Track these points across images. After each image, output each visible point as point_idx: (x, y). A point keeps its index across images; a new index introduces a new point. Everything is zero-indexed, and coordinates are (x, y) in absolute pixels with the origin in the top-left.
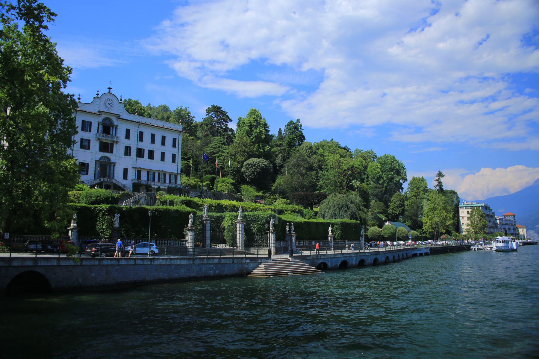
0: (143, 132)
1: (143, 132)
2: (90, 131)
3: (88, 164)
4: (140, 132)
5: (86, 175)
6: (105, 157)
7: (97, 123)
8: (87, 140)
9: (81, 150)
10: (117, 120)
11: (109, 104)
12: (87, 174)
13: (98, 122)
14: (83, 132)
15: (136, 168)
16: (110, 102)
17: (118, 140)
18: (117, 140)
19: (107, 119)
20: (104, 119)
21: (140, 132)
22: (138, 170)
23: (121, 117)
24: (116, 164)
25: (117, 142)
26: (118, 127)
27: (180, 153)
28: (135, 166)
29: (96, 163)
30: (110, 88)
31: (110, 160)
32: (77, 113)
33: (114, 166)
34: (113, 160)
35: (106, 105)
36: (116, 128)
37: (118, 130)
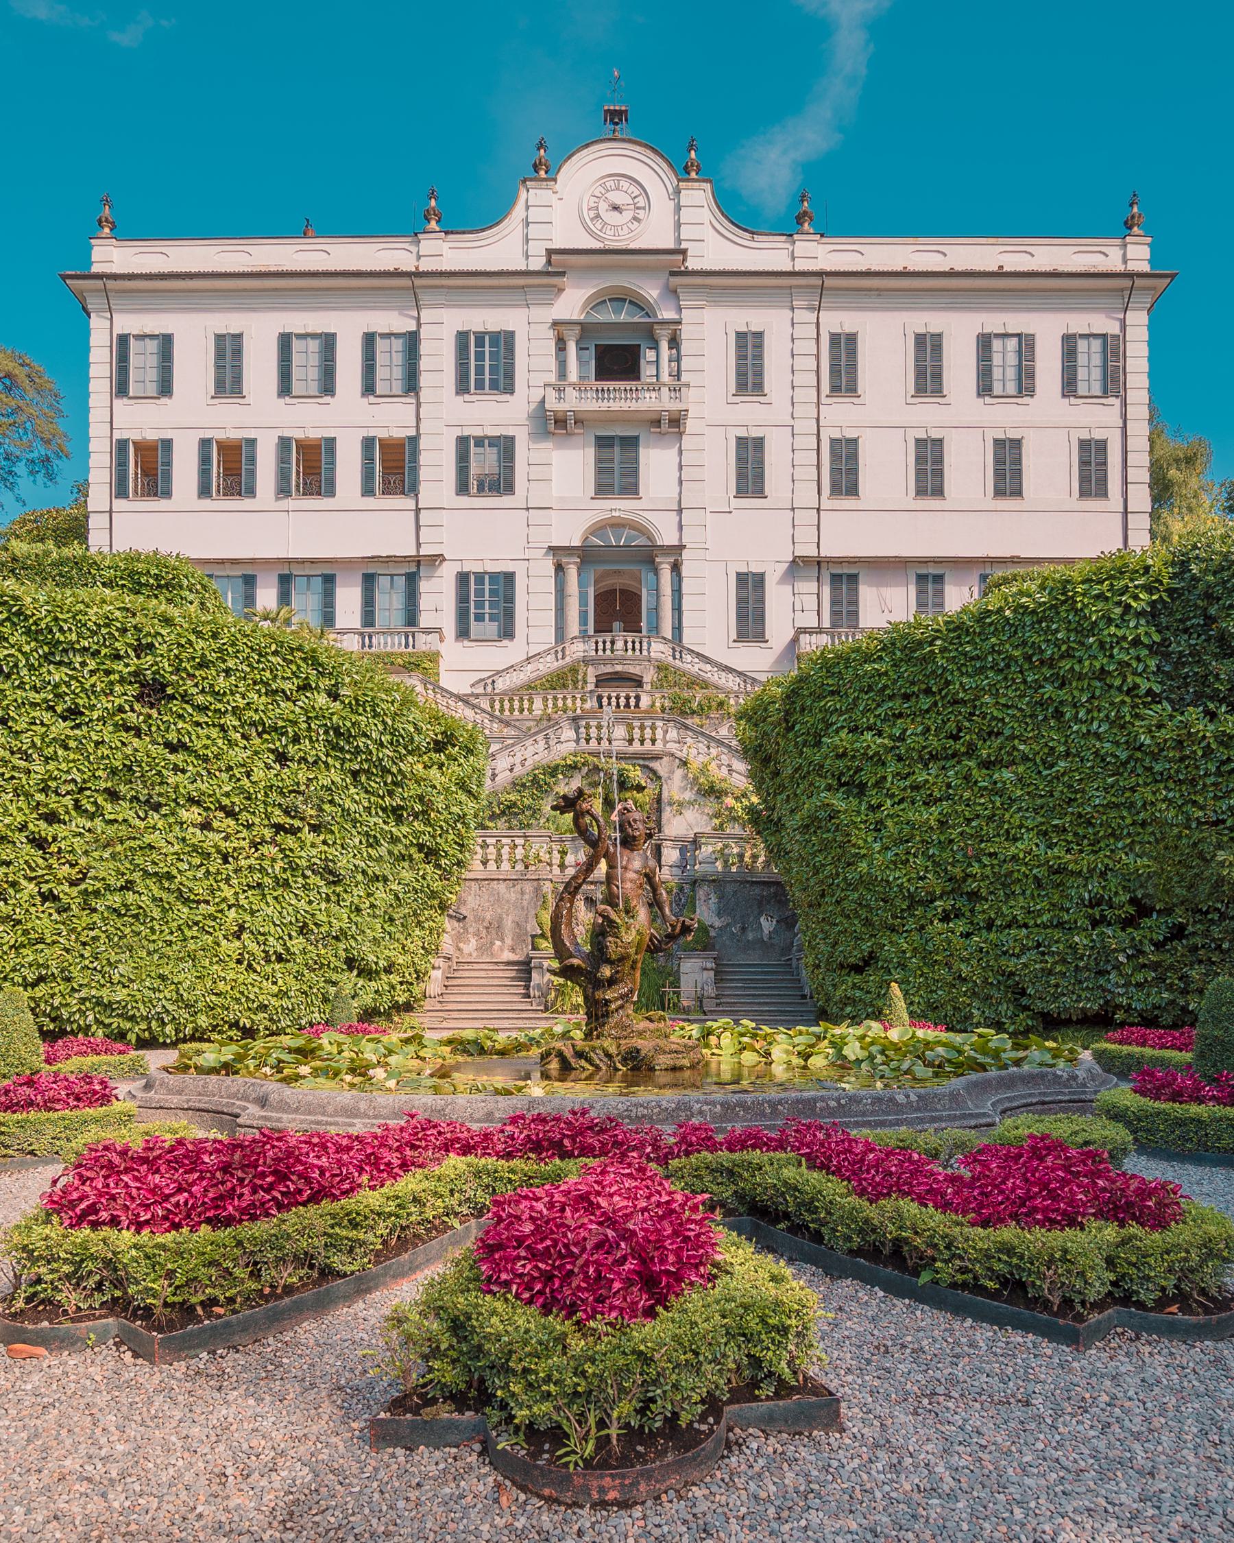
0: (852, 338)
1: (852, 338)
2: (509, 389)
3: (509, 577)
4: (835, 338)
5: (506, 642)
6: (617, 525)
7: (551, 334)
8: (494, 441)
9: (464, 501)
10: (673, 293)
11: (616, 208)
12: (507, 632)
13: (555, 324)
14: (467, 398)
15: (819, 563)
16: (618, 198)
17: (681, 407)
18: (674, 406)
19: (620, 298)
20: (597, 302)
21: (835, 338)
22: (833, 576)
23: (692, 264)
24: (686, 554)
25: (676, 421)
26: (686, 332)
27: (1140, 430)
28: (812, 552)
29: (559, 568)
30: (616, 117)
31: (650, 538)
32: (424, 298)
33: (676, 567)
34: (668, 537)
35: (598, 216)
36: (674, 342)
37: (685, 348)
